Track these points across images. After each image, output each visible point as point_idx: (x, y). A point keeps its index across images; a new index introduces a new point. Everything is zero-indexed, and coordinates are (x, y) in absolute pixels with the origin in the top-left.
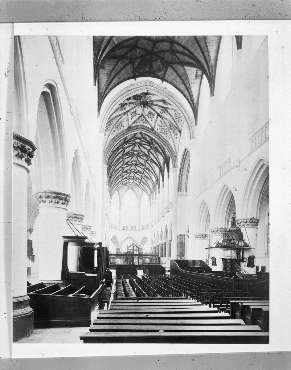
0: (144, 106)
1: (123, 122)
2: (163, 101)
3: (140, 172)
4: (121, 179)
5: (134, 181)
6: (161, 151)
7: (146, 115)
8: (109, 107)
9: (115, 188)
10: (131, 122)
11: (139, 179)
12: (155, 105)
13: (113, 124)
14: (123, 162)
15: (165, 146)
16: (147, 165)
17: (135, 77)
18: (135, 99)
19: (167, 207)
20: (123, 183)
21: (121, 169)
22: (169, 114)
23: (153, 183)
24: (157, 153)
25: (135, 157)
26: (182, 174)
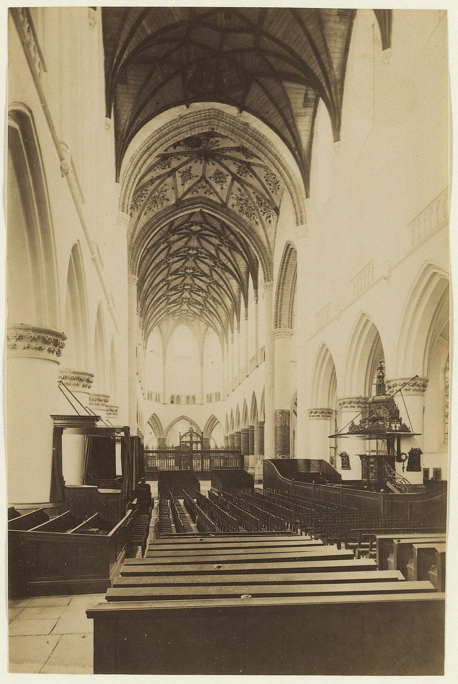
0: (207, 160)
2: (242, 149)
3: (203, 290)
5: (189, 308)
6: (241, 249)
7: (210, 178)
8: (139, 161)
9: (154, 321)
10: (181, 190)
11: (200, 304)
12: (227, 158)
14: (167, 269)
16: (216, 277)
17: (187, 102)
19: (255, 358)
21: (164, 283)
26: (282, 294)
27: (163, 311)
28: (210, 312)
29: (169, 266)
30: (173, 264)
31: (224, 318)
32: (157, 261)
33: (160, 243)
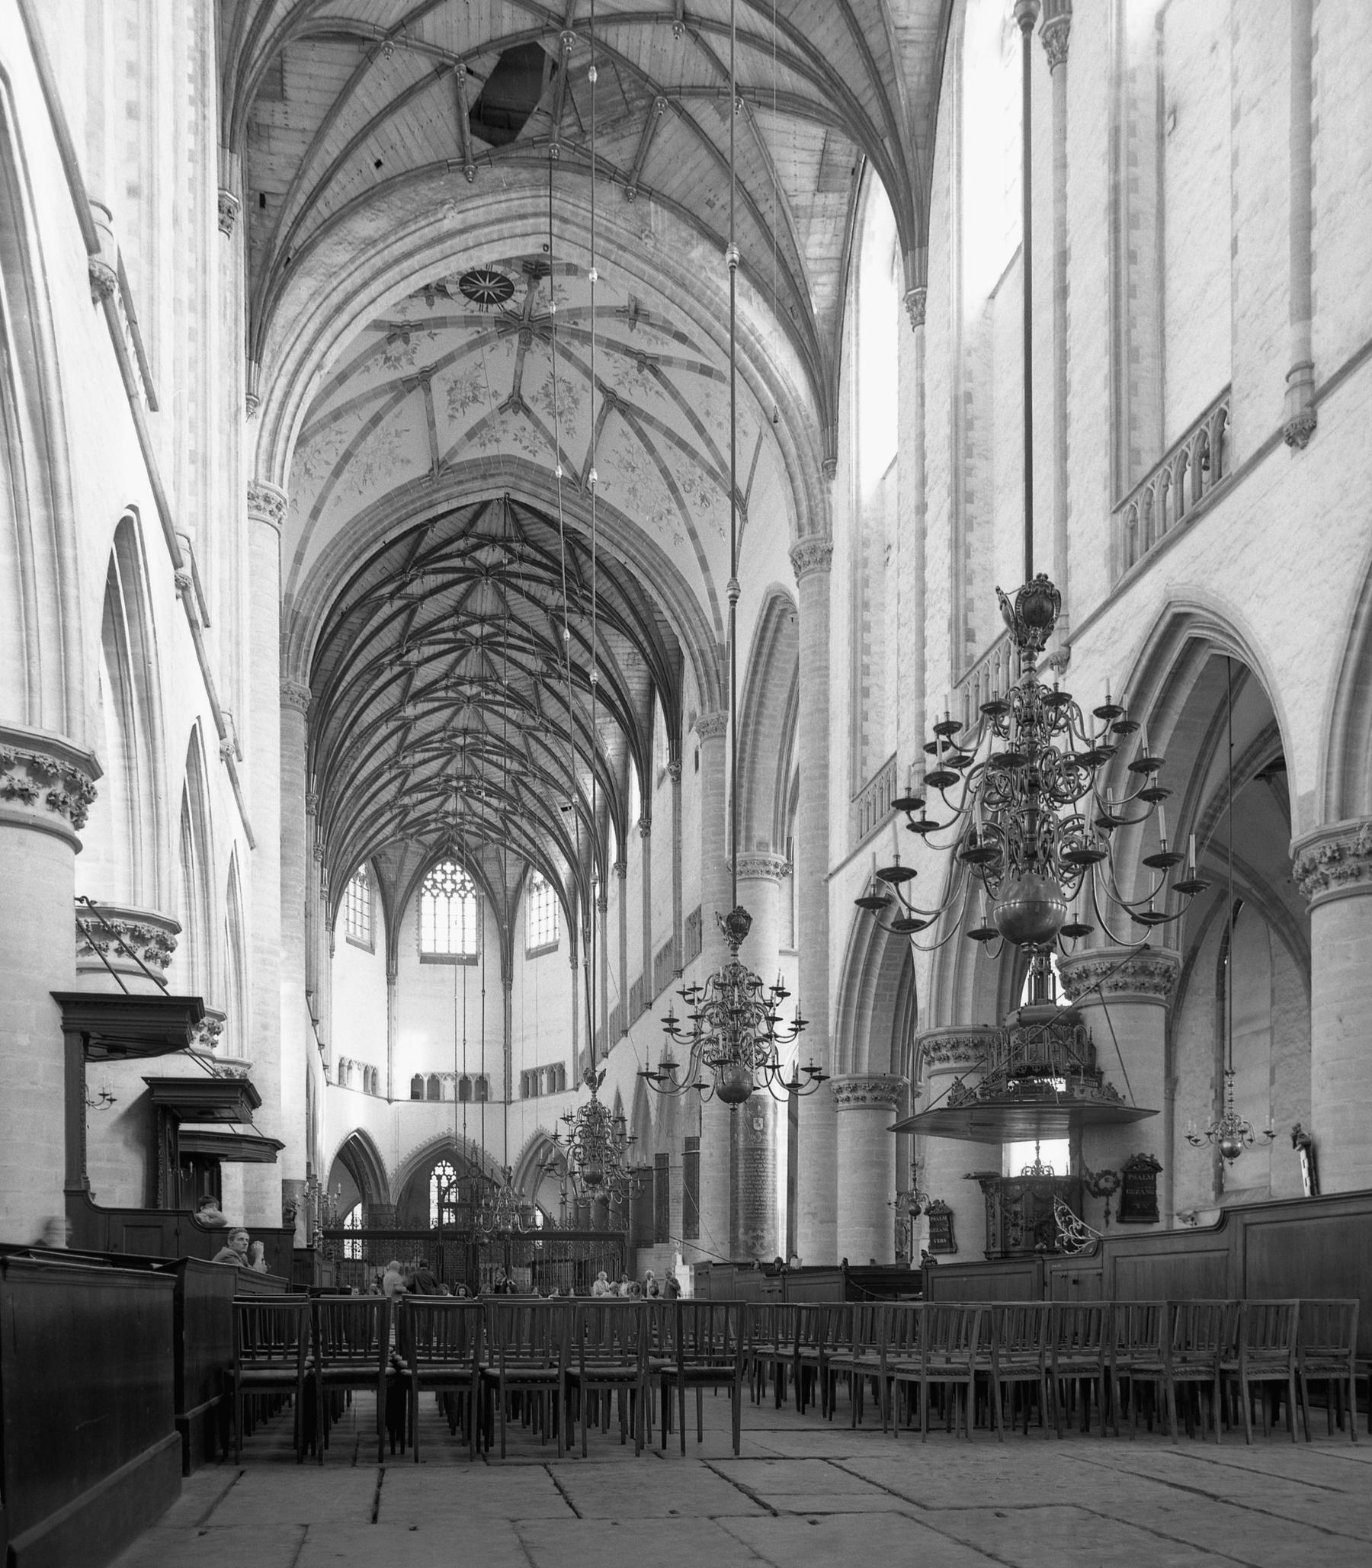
2: (634, 314)
3: (510, 751)
4: (393, 788)
6: (631, 620)
7: (534, 399)
12: (586, 338)
13: (338, 445)
14: (401, 682)
16: (552, 708)
18: (470, 295)
20: (408, 819)
21: (393, 725)
24: (608, 631)
27: (388, 816)
30: (419, 664)
33: (382, 597)
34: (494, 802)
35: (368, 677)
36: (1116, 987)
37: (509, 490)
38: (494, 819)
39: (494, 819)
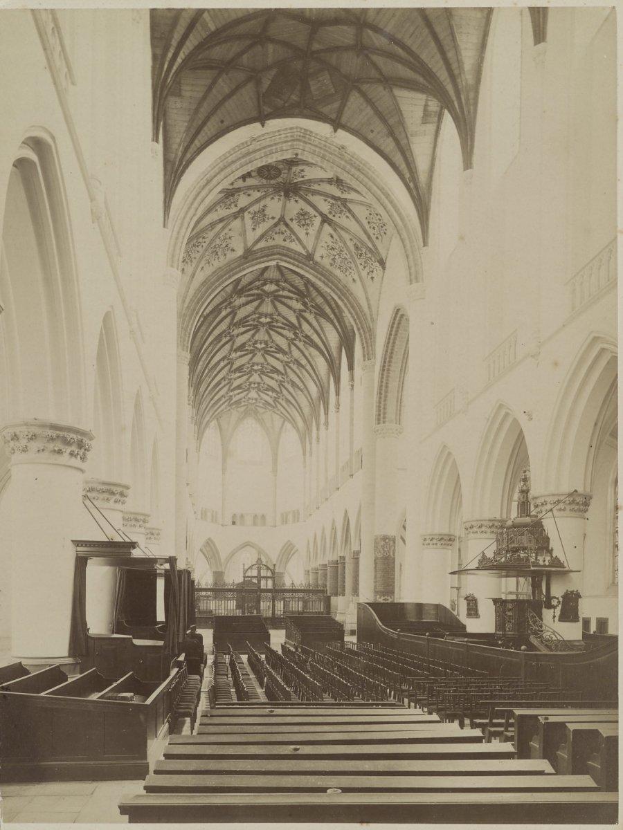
0: (287, 196)
1: (230, 238)
2: (338, 182)
3: (277, 371)
4: (225, 389)
5: (259, 396)
6: (332, 316)
7: (291, 220)
8: (195, 199)
9: (211, 414)
10: (252, 237)
11: (273, 390)
12: (315, 193)
14: (230, 343)
15: (342, 300)
17: (262, 118)
18: (262, 177)
20: (232, 401)
21: (226, 362)
22: (354, 216)
23: (311, 398)
24: (322, 320)
25: (263, 330)
26: (388, 376)
27: (223, 400)
28: (288, 401)
29: (232, 339)
30: (238, 336)
31: (306, 410)
32: (216, 332)
34: (270, 393)
35: (215, 342)
36: (560, 510)
37: (279, 261)
38: (271, 401)
39: (271, 401)
